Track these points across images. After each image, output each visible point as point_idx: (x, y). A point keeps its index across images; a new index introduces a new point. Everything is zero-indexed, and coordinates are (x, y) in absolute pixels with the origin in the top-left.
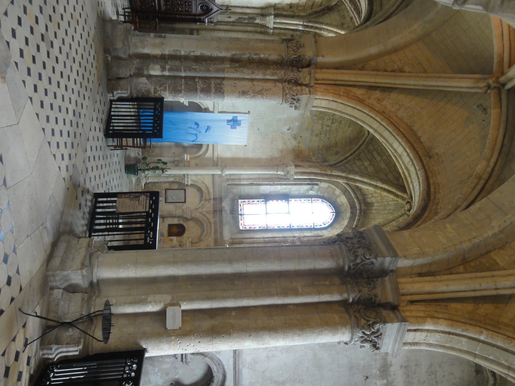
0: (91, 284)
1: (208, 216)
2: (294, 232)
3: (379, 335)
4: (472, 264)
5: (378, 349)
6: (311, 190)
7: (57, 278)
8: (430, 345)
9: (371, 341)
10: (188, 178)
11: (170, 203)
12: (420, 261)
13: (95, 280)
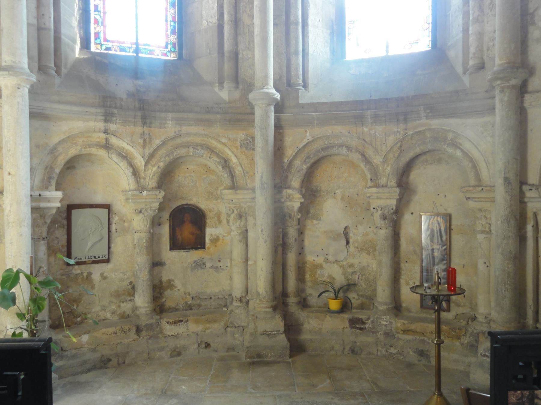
1: (157, 142)
11: (109, 248)
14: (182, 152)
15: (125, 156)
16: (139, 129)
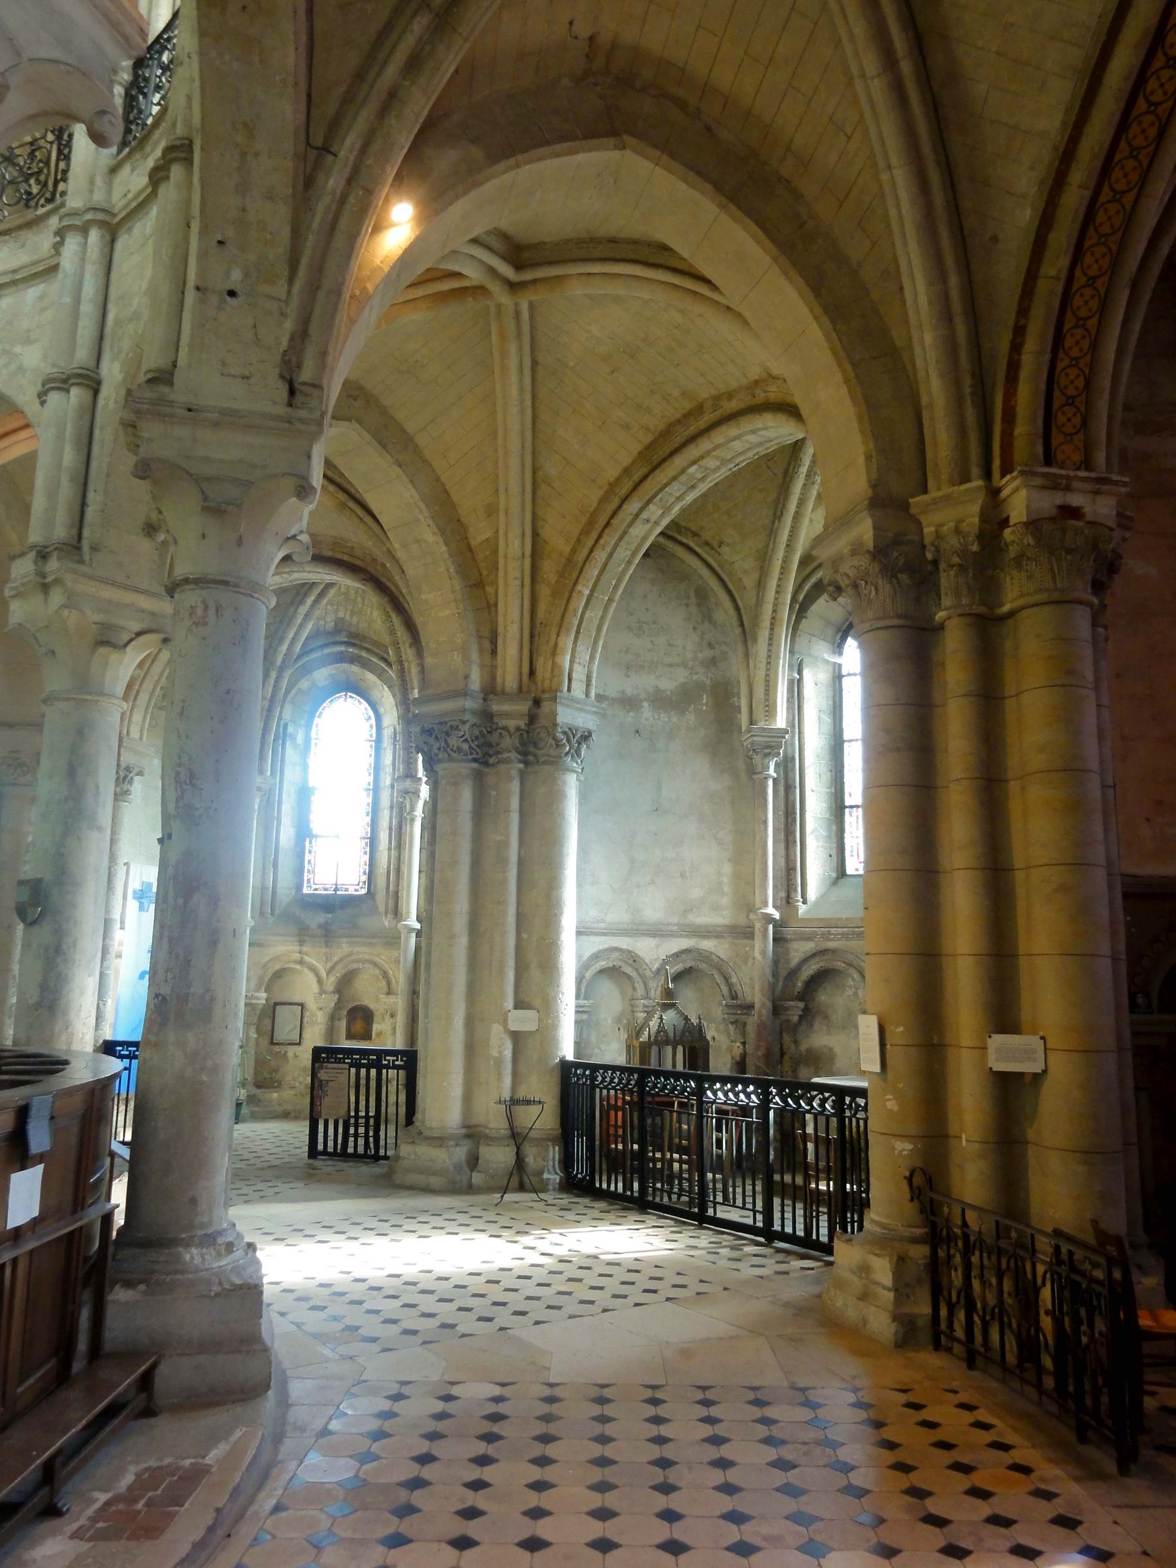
0: (468, 1136)
1: (336, 959)
2: (382, 785)
3: (570, 732)
4: (485, 573)
5: (590, 734)
6: (295, 739)
7: (458, 1178)
8: (592, 658)
9: (579, 743)
10: (253, 997)
11: (301, 1035)
12: (475, 656)
13: (464, 1131)
14: (355, 966)
15: (313, 969)
16: (324, 950)
